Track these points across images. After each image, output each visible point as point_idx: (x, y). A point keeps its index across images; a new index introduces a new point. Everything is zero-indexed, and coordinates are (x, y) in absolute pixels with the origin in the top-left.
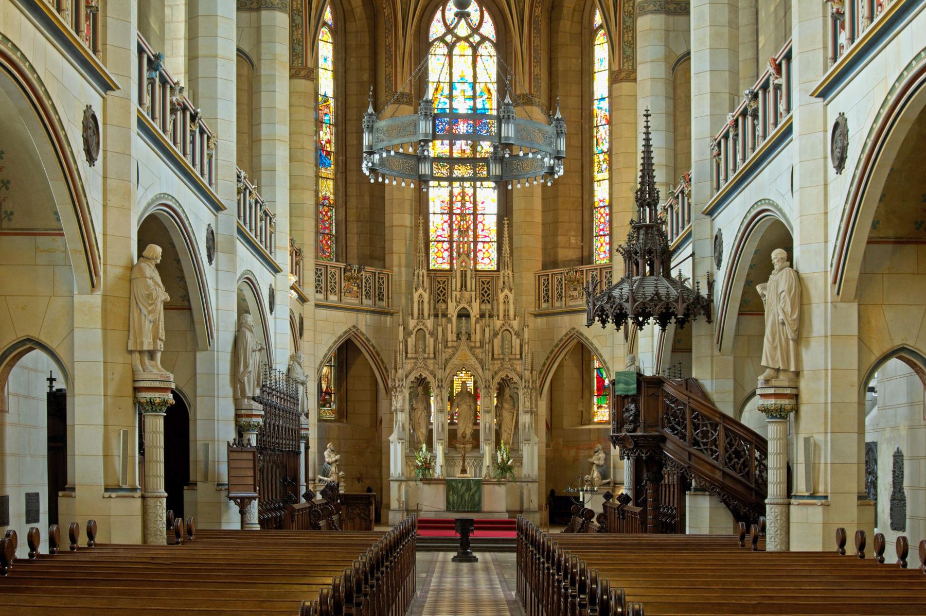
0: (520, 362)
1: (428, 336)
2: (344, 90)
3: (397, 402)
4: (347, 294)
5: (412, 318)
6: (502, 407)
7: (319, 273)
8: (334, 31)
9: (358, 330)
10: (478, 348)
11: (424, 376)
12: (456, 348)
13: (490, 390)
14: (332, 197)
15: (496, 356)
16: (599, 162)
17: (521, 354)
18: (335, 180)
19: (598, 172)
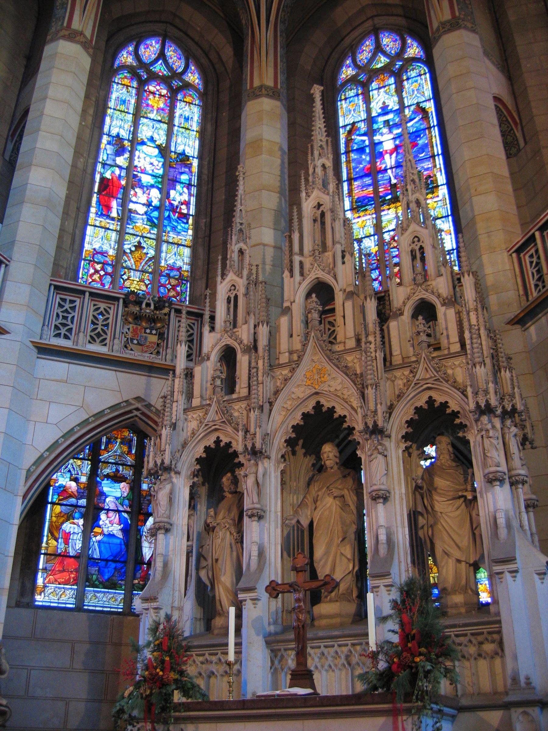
0: (463, 359)
2: (213, 147)
4: (131, 346)
6: (431, 489)
7: (67, 306)
8: (203, 96)
9: (149, 406)
14: (186, 268)
15: (397, 360)
18: (194, 247)
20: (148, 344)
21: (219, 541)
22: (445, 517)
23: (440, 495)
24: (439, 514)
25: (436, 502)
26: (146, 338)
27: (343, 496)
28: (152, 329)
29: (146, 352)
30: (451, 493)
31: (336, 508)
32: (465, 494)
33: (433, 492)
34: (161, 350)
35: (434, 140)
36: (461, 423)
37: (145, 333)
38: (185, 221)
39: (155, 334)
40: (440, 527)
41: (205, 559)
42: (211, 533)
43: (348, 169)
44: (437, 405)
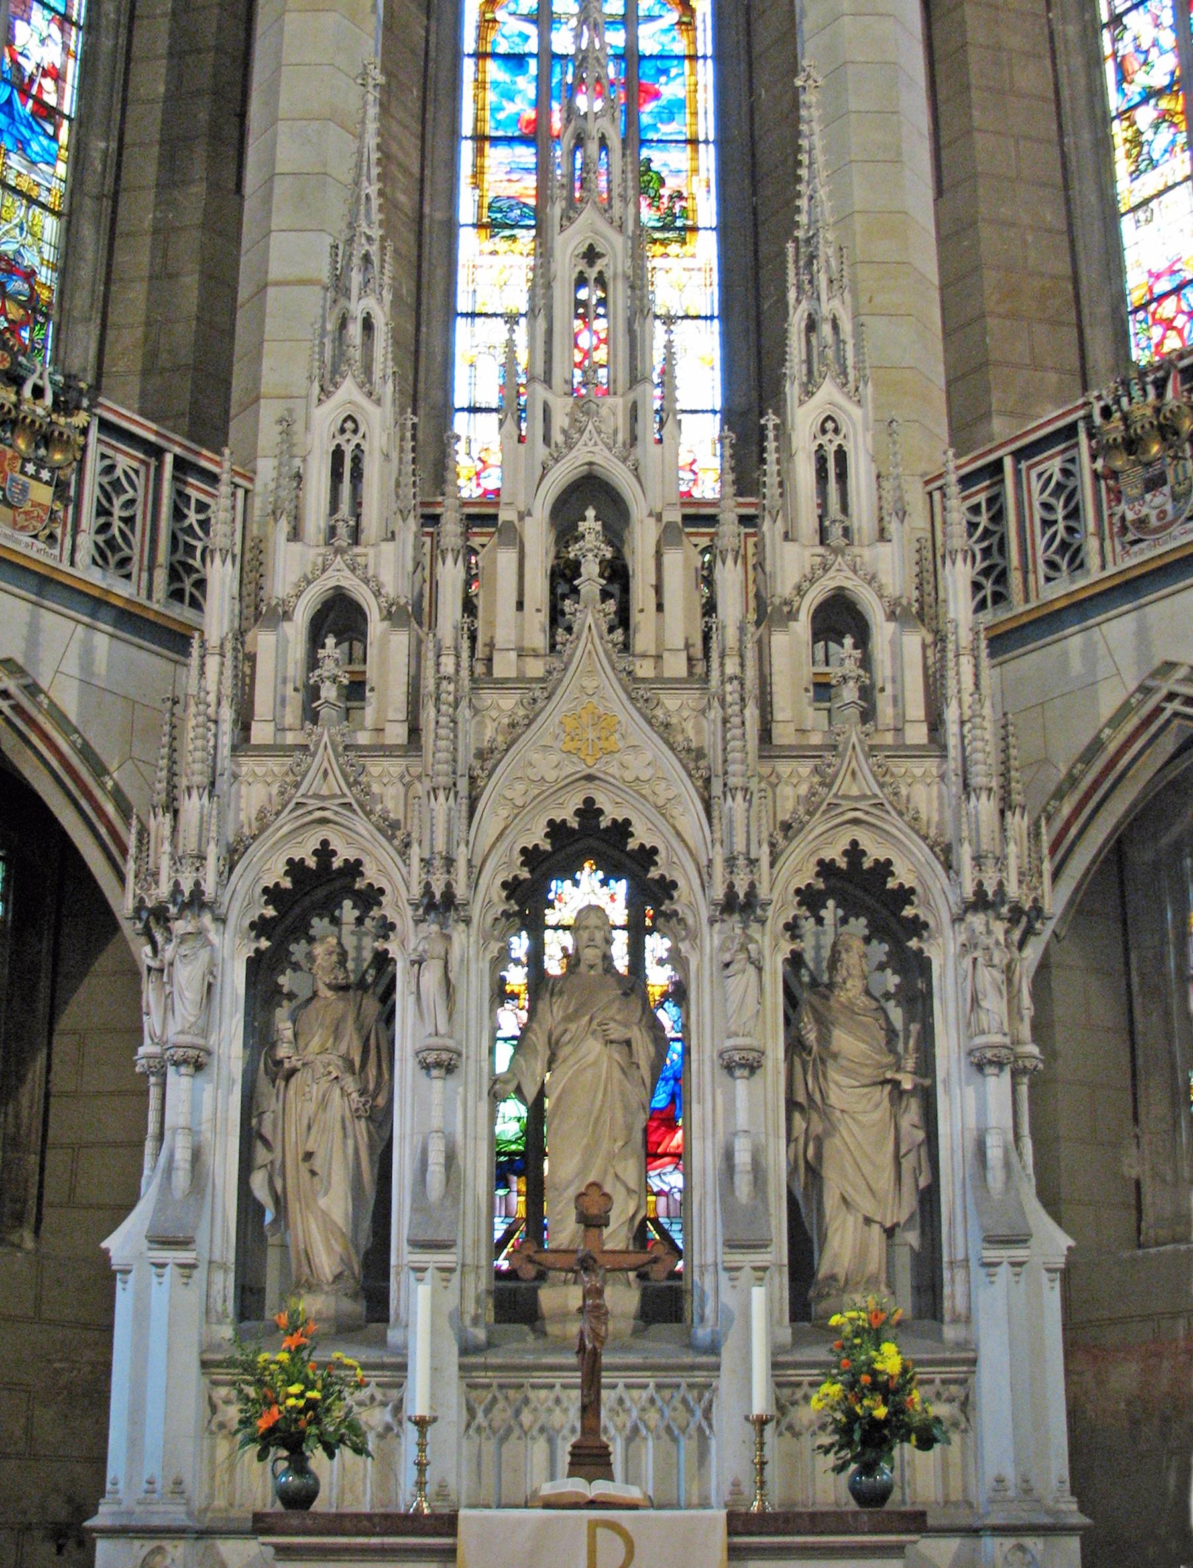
1: (376, 626)
3: (169, 1009)
5: (295, 535)
10: (674, 684)
11: (344, 852)
12: (549, 685)
13: (754, 929)
16: (1136, 141)
17: (935, 723)
19: (1136, 174)
20: (27, 507)
21: (311, 1107)
22: (849, 1121)
23: (847, 1072)
24: (838, 1113)
25: (832, 1085)
26: (25, 490)
27: (628, 1043)
28: (40, 463)
29: (23, 528)
30: (867, 1071)
31: (610, 1067)
32: (898, 1077)
33: (830, 1063)
34: (59, 532)
35: (700, 96)
36: (916, 916)
37: (23, 472)
38: (50, 130)
39: (47, 483)
40: (837, 1141)
41: (267, 1143)
42: (281, 1083)
43: (479, 109)
44: (867, 864)
